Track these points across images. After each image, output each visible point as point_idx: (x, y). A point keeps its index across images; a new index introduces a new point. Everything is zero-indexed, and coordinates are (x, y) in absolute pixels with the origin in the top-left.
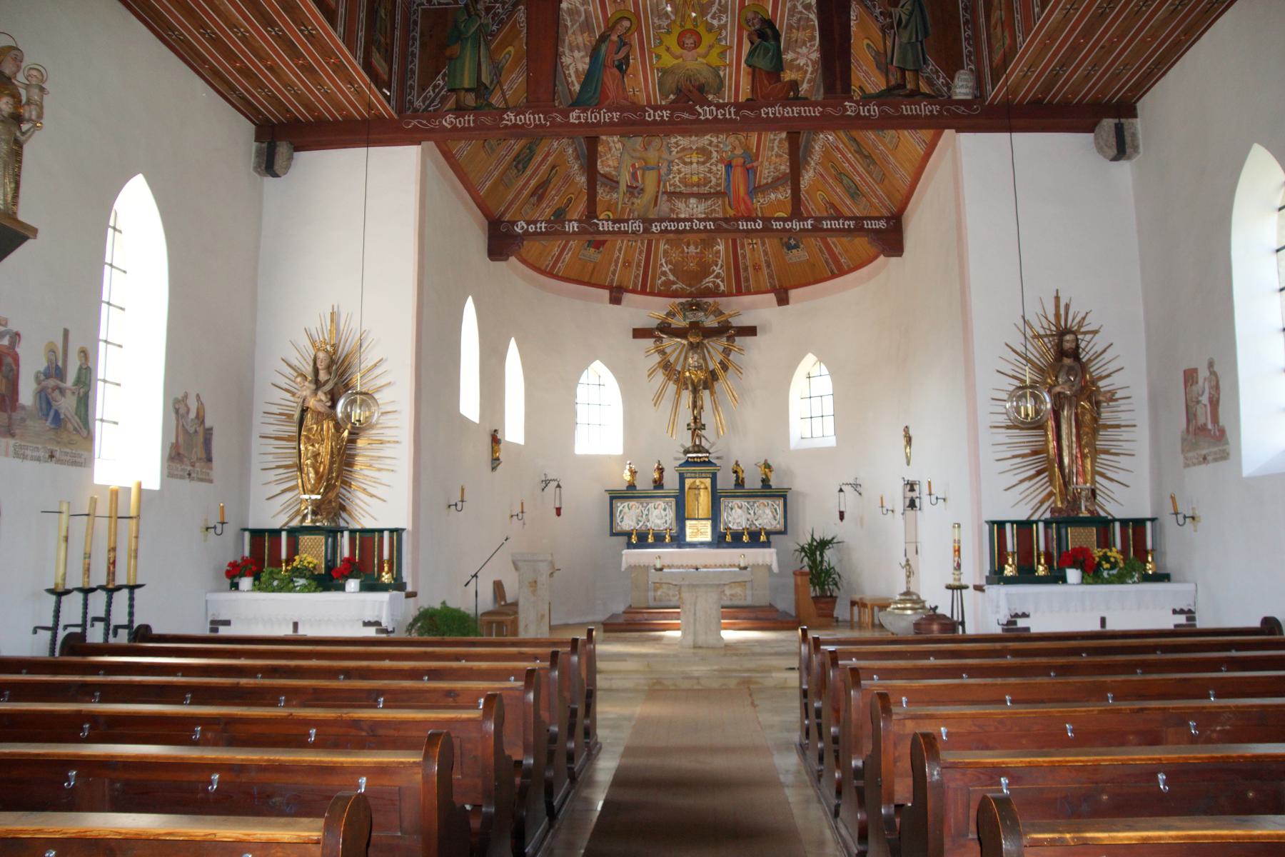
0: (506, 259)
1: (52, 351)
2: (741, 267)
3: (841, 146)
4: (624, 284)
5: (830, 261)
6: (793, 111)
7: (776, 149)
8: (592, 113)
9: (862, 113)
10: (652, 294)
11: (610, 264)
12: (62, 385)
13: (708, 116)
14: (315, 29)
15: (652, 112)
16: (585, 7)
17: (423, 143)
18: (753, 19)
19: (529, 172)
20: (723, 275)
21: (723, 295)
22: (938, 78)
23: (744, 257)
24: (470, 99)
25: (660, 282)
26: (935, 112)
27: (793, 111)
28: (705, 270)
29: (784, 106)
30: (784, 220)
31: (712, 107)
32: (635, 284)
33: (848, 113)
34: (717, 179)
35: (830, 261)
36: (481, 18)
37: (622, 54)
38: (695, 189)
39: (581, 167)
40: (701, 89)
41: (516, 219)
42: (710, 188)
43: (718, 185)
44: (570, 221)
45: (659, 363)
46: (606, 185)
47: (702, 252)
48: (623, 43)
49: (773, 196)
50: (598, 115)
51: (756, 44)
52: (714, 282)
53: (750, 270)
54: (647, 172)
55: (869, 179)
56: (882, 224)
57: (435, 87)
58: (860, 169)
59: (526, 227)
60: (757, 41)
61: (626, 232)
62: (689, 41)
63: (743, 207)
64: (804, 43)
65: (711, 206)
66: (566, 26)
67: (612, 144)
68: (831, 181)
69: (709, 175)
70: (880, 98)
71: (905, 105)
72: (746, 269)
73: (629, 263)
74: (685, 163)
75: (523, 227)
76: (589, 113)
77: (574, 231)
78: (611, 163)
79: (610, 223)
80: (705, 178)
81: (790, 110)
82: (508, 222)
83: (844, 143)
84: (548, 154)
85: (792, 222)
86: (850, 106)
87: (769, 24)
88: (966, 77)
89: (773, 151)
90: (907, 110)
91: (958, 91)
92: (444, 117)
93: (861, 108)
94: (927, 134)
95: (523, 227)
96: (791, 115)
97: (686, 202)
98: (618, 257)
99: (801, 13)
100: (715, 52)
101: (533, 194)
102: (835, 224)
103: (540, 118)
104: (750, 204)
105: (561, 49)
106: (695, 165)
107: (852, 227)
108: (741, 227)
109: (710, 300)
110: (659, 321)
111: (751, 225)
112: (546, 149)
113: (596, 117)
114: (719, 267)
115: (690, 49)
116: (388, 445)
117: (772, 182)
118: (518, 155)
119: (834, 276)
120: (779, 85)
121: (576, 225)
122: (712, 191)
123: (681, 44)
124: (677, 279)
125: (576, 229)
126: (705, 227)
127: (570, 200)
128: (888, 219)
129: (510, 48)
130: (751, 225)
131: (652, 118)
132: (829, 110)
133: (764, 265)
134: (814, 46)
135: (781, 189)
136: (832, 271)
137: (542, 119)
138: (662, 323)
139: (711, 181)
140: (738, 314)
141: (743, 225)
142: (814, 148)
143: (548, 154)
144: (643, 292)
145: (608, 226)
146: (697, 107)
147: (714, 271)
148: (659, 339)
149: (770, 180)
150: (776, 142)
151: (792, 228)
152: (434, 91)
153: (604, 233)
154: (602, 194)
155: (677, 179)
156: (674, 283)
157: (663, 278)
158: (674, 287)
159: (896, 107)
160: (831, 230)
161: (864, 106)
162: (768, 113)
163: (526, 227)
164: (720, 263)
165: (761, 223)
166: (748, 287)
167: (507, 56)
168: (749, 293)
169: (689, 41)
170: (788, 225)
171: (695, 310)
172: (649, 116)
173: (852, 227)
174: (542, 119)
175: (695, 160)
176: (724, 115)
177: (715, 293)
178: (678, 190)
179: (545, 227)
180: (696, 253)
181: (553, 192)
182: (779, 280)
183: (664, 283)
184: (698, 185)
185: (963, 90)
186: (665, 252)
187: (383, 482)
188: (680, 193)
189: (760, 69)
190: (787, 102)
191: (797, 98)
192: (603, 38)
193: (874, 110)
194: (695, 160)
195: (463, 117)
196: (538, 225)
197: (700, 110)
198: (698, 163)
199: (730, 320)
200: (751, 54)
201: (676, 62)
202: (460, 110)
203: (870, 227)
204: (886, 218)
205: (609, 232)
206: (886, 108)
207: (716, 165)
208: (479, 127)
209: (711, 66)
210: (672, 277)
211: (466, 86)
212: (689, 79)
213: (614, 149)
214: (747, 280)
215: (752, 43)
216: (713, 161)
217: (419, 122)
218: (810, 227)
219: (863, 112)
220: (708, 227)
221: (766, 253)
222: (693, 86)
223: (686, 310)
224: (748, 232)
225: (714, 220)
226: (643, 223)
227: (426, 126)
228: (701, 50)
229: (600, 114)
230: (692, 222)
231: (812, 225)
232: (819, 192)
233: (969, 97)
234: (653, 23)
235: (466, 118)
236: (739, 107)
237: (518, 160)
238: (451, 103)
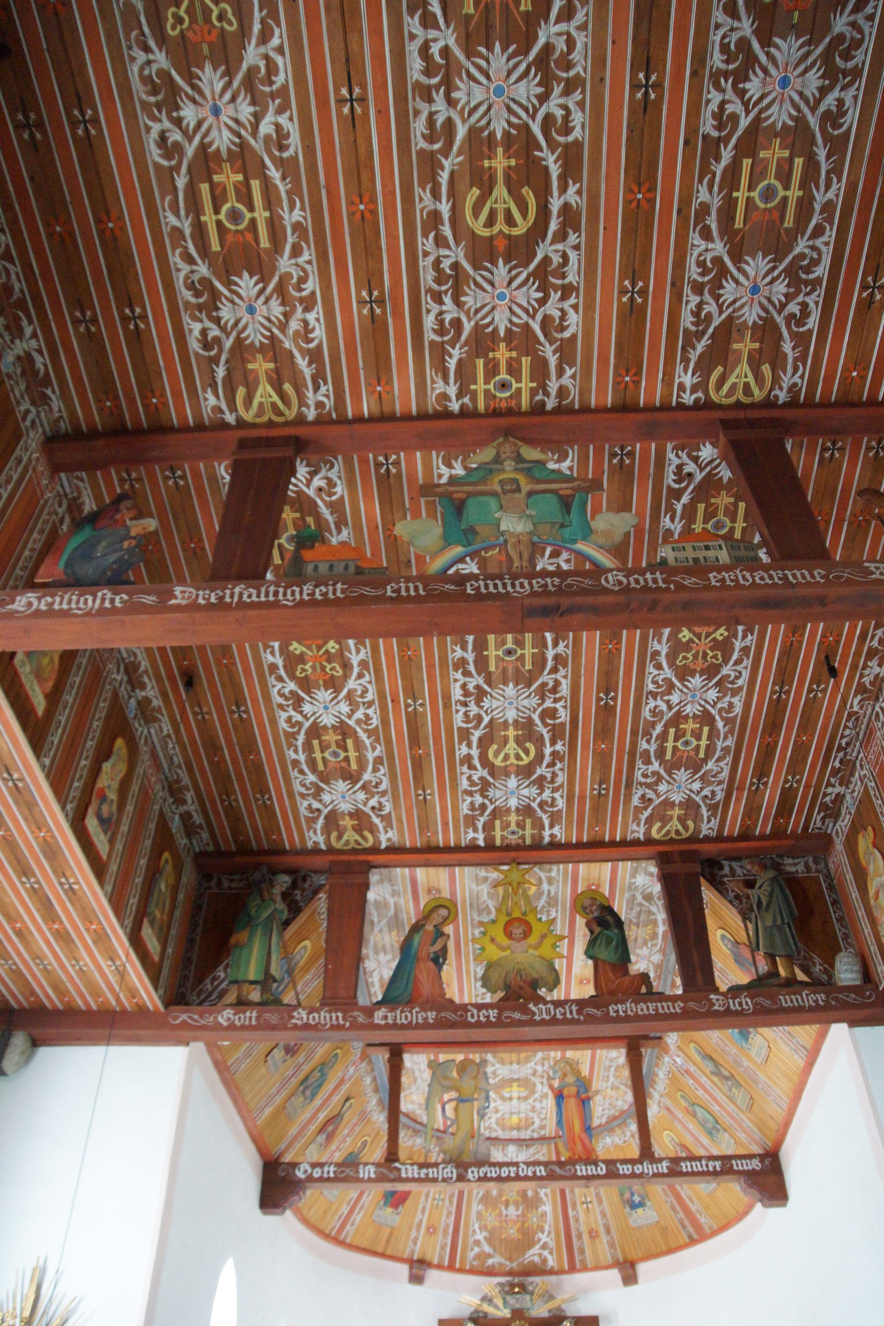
0: (282, 1213)
2: (574, 1233)
3: (693, 1068)
4: (428, 1258)
5: (687, 1222)
6: (648, 1007)
7: (612, 1079)
8: (402, 1012)
9: (732, 1007)
10: (461, 1270)
11: (410, 1229)
13: (544, 1016)
14: (78, 883)
15: (475, 1011)
16: (396, 899)
17: (191, 1044)
18: (592, 905)
19: (318, 1102)
20: (552, 1244)
21: (551, 1272)
22: (814, 964)
23: (577, 1220)
24: (255, 995)
26: (821, 1002)
27: (648, 1007)
28: (528, 1239)
29: (637, 1002)
30: (633, 1162)
31: (549, 1006)
32: (441, 1258)
33: (716, 1008)
34: (542, 1120)
35: (687, 1222)
36: (275, 903)
37: (438, 947)
38: (515, 1134)
39: (380, 1102)
40: (534, 984)
41: (297, 1161)
42: (533, 1131)
43: (542, 1127)
44: (366, 1164)
46: (409, 1128)
47: (523, 1215)
48: (439, 933)
49: (608, 1140)
50: (409, 1015)
51: (596, 933)
52: (540, 1255)
53: (585, 1236)
54: (461, 1105)
55: (731, 1107)
56: (755, 1164)
57: (214, 979)
58: (719, 1095)
59: (309, 1171)
60: (598, 929)
61: (435, 1180)
62: (518, 931)
63: (579, 1147)
64: (645, 943)
65: (534, 1155)
66: (372, 923)
67: (417, 1074)
68: (680, 1116)
69: (531, 1114)
70: (751, 988)
71: (784, 995)
72: (580, 1236)
73: (435, 1229)
74: (503, 1099)
75: (306, 1171)
76: (398, 1012)
78: (415, 1098)
79: (415, 1167)
80: (526, 1119)
81: (644, 1007)
82: (288, 1164)
83: (695, 1064)
84: (342, 1082)
85: (642, 1164)
86: (717, 1000)
87: (609, 910)
88: (846, 960)
89: (608, 1081)
90: (786, 1000)
91: (843, 976)
92: (220, 1012)
93: (731, 1001)
94: (812, 1030)
95: (306, 1171)
96: (646, 1012)
97: (503, 1150)
98: (421, 1221)
99: (641, 905)
100: (548, 942)
101: (321, 1130)
102: (697, 1166)
103: (337, 1018)
104: (587, 1141)
105: (364, 951)
106: (515, 1102)
107: (718, 1169)
108: (579, 1173)
109: (537, 1279)
110: (472, 1309)
111: (591, 1170)
112: (340, 1074)
113: (406, 1017)
114: (546, 1233)
115: (519, 940)
117: (607, 1123)
118: (306, 1079)
119: (693, 1242)
120: (627, 978)
122: (535, 1135)
123: (509, 935)
124: (495, 1250)
125: (373, 1175)
126: (534, 1172)
127: (365, 1144)
128: (762, 1157)
129: (307, 943)
130: (591, 1170)
131: (476, 1019)
132: (692, 1005)
133: (602, 1231)
134: (656, 945)
135: (618, 1131)
136: (690, 1236)
137: (340, 1018)
138: (476, 1311)
139: (533, 1123)
140: (573, 1299)
141: (581, 1170)
142: (656, 1075)
143: (342, 1082)
144: (451, 1268)
145: (412, 1171)
146: (531, 1006)
147: (539, 1240)
149: (604, 1120)
150: (612, 1069)
151: (643, 1173)
152: (212, 984)
153: (407, 1180)
154: (405, 1139)
155: (493, 1120)
156: (490, 1256)
158: (490, 1262)
159: (773, 998)
160: (693, 1174)
161: (734, 998)
162: (617, 1011)
163: (309, 1171)
164: (547, 1229)
165: (604, 1167)
166: (583, 1262)
167: (303, 952)
168: (585, 1269)
169: (518, 931)
170: (638, 1169)
171: (518, 1293)
172: (472, 1016)
173: (718, 1169)
174: (340, 1018)
175: (515, 1095)
176: (565, 1014)
177: (540, 1270)
178: (494, 1135)
179: (335, 1172)
180: (517, 1216)
181: (346, 1132)
182: (624, 1252)
183: (478, 1257)
184: (518, 1128)
185: (849, 976)
186: (479, 1216)
188: (496, 1139)
189: (604, 961)
190: (638, 998)
191: (650, 992)
192: (416, 928)
193: (747, 1003)
194: (515, 1095)
195: (244, 1012)
196: (326, 1169)
197: (534, 1009)
198: (519, 1098)
199: (564, 1307)
200: (592, 944)
201: (503, 954)
202: (242, 1004)
203: (740, 1168)
204: (759, 1155)
205: (413, 1180)
206: (760, 1000)
207: (541, 1102)
208: (263, 1026)
209: (543, 958)
210: (487, 1249)
211: (252, 976)
212: (519, 972)
213: (419, 1080)
214: (582, 1251)
215: (592, 932)
216: (537, 1095)
217: (190, 1017)
218: (665, 1171)
219: (734, 1005)
220: (538, 1174)
221: (604, 1215)
222: (525, 982)
223: (507, 1293)
224: (589, 1178)
225: (546, 1164)
226: (457, 1167)
227: (196, 1021)
228: (533, 939)
229: (411, 1012)
230: (518, 1167)
231: (668, 1168)
232: (666, 1132)
233: (858, 983)
234: (472, 920)
235: (248, 1014)
236: (581, 1004)
237: (305, 1084)
238: (231, 997)
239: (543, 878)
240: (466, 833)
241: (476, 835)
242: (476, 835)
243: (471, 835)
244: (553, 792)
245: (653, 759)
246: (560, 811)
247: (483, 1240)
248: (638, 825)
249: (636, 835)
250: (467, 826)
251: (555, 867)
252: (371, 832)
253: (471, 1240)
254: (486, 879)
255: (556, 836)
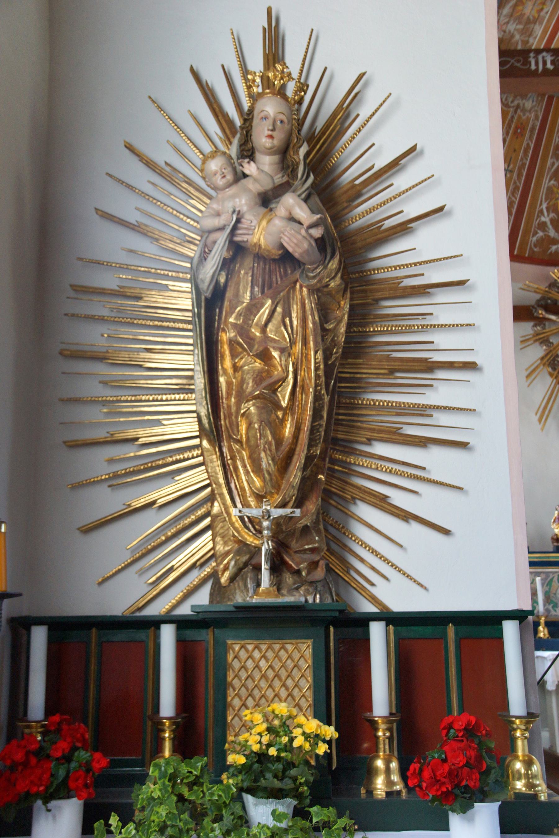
25: (534, 239)
45: (542, 358)
77: (545, 70)
110: (538, 296)
116: (441, 374)
121: (549, 59)
125: (549, 66)
138: (543, 298)
148: (540, 321)
157: (540, 234)
186: (550, 190)
187: (433, 477)
210: (552, 233)
247: (549, 223)
253: (536, 223)
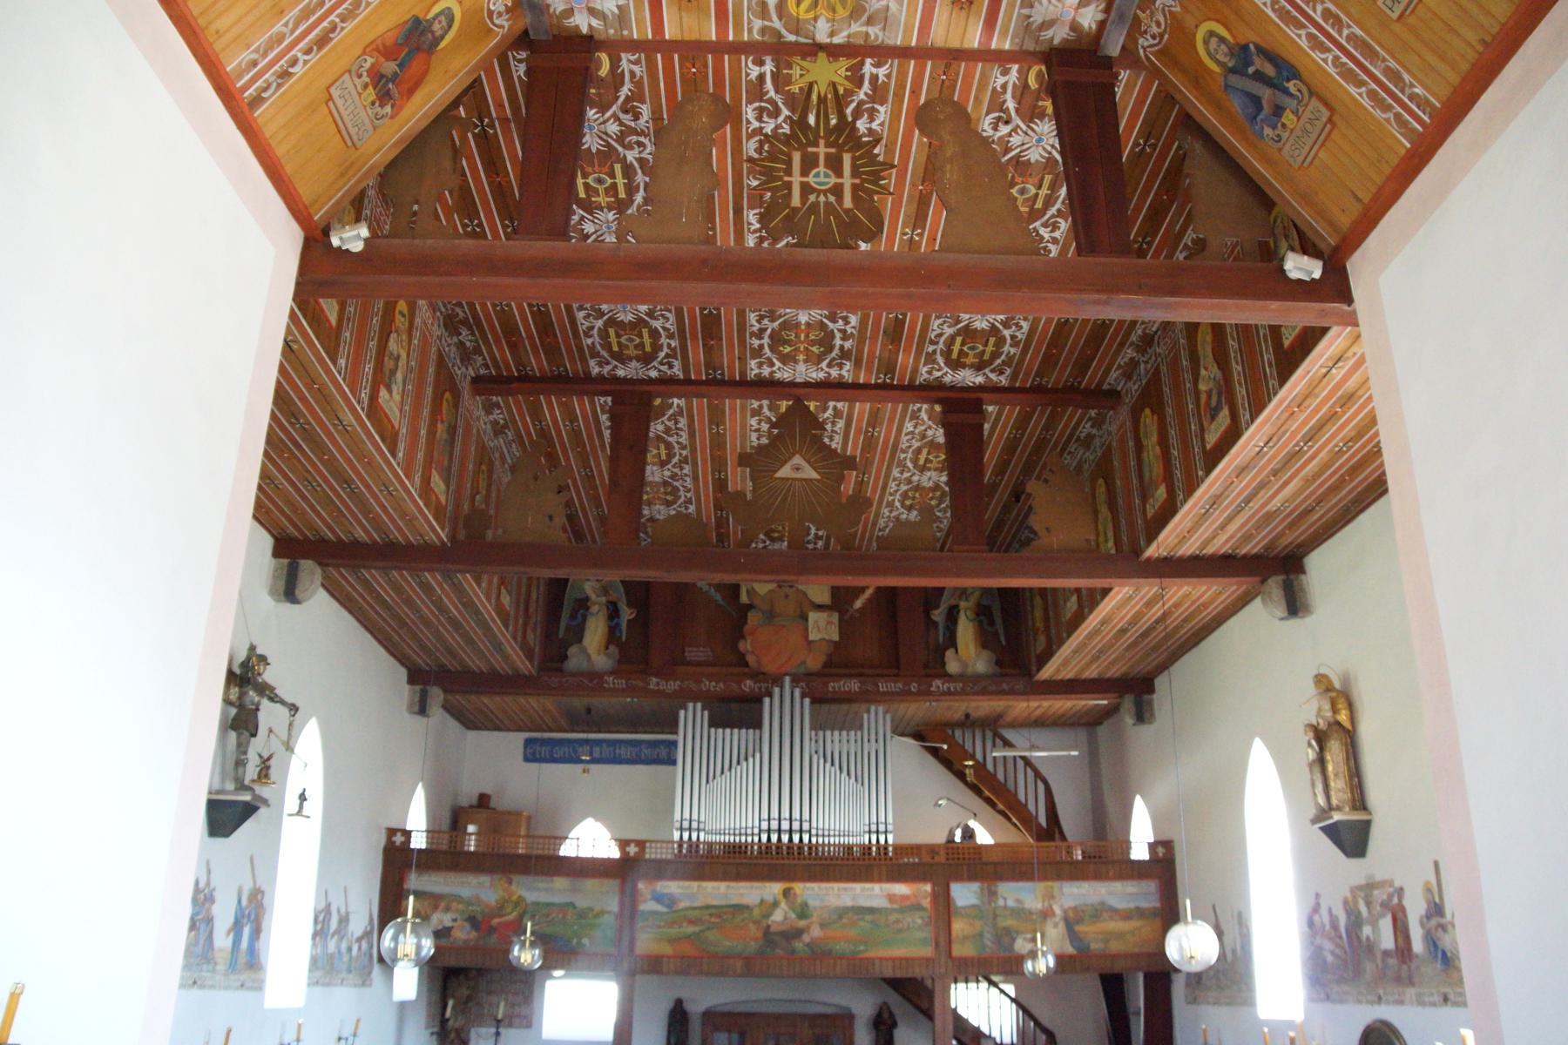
1: (1428, 890)
12: (1442, 921)
239: (775, 18)
240: (888, 76)
241: (874, 71)
242: (874, 71)
243: (882, 72)
244: (761, 129)
245: (636, 165)
246: (749, 102)
248: (632, 74)
249: (632, 58)
250: (886, 85)
251: (757, 37)
252: (1026, 86)
254: (870, 22)
255: (754, 63)
